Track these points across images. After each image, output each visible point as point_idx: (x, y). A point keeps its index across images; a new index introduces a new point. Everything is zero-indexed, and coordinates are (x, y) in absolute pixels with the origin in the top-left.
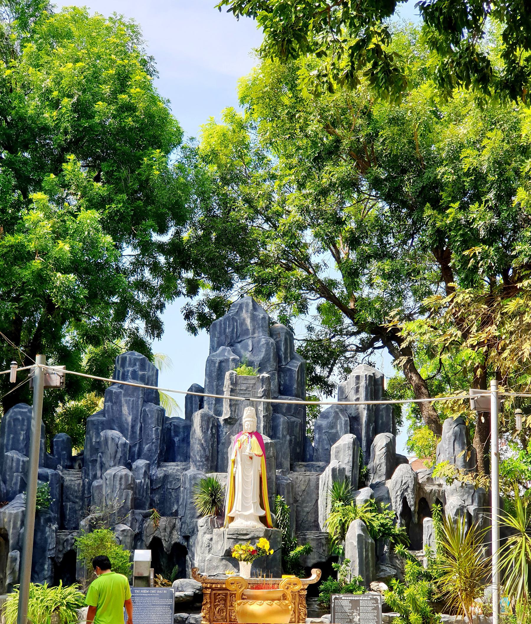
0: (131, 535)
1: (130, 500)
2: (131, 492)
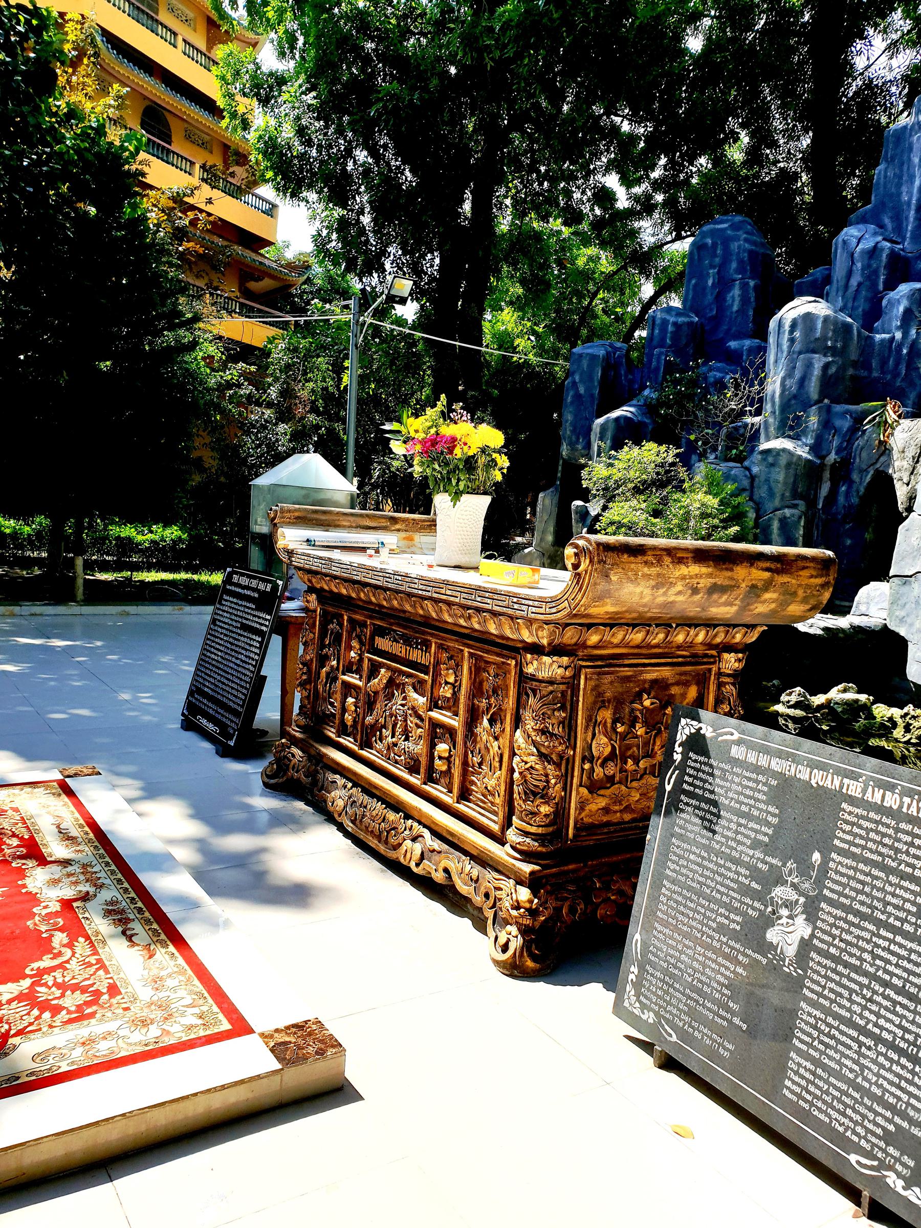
0: (788, 465)
1: (814, 379)
2: (819, 361)
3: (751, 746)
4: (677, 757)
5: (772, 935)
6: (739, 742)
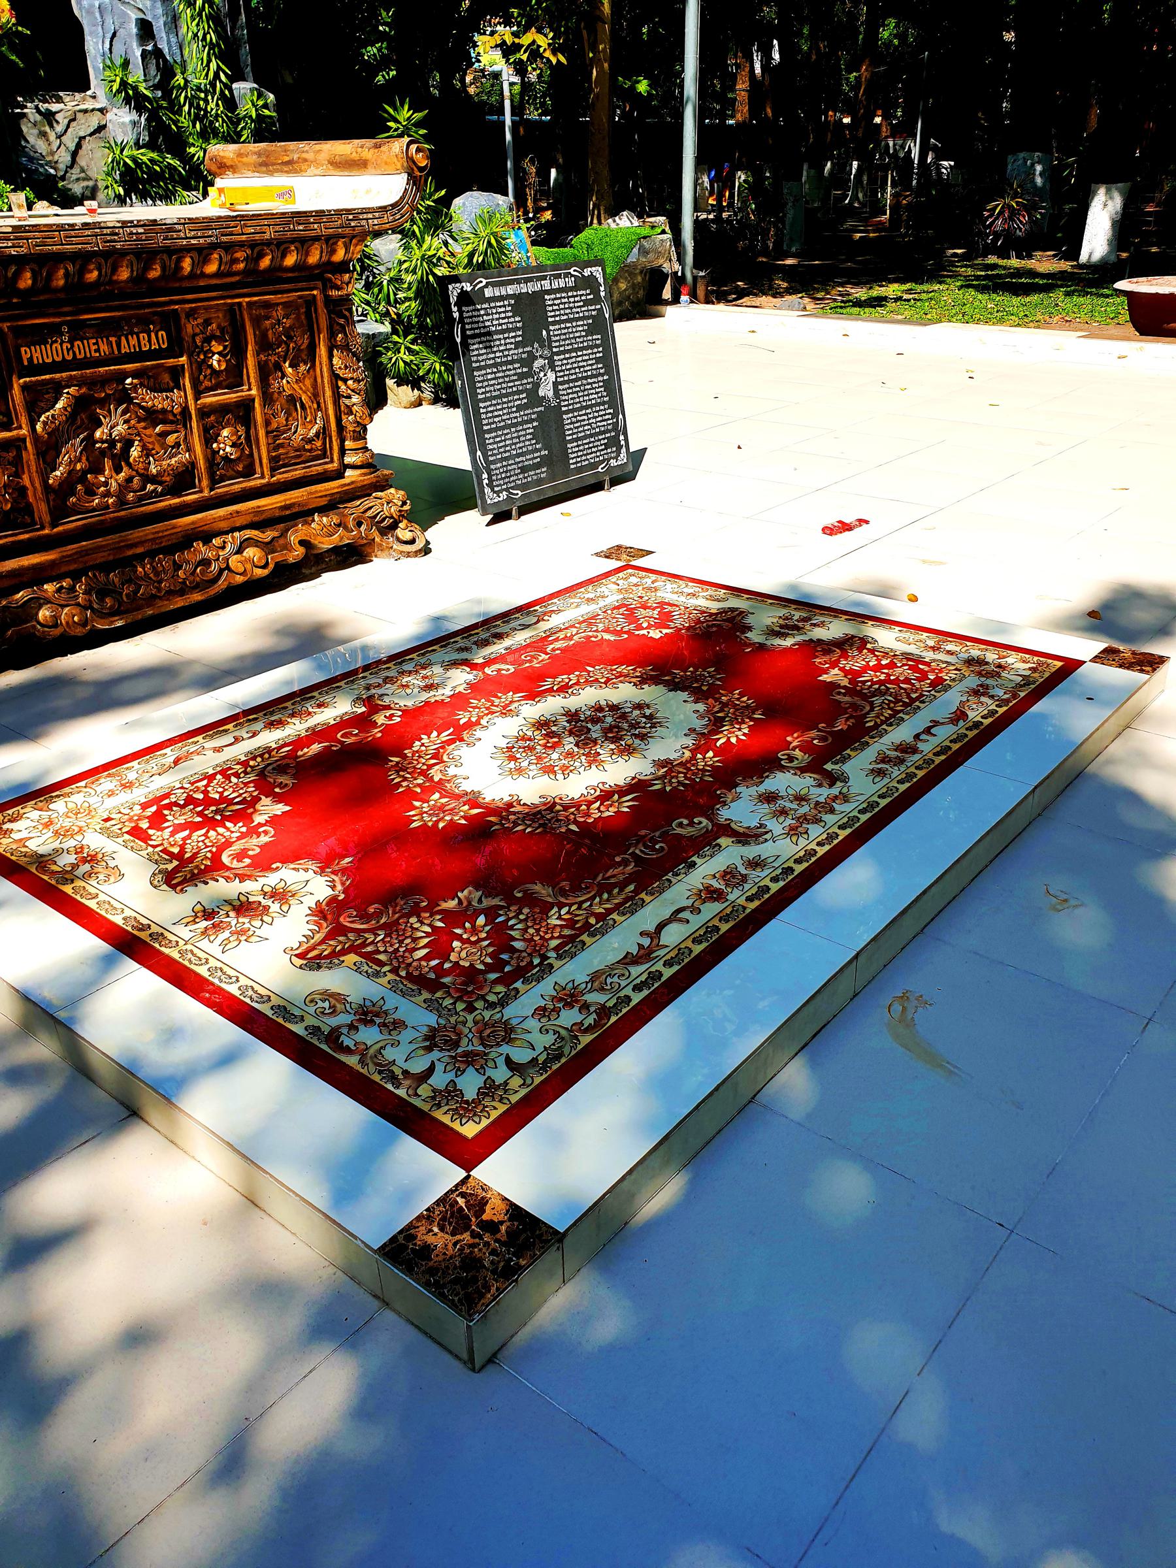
3: (494, 285)
4: (456, 315)
5: (541, 393)
6: (486, 286)
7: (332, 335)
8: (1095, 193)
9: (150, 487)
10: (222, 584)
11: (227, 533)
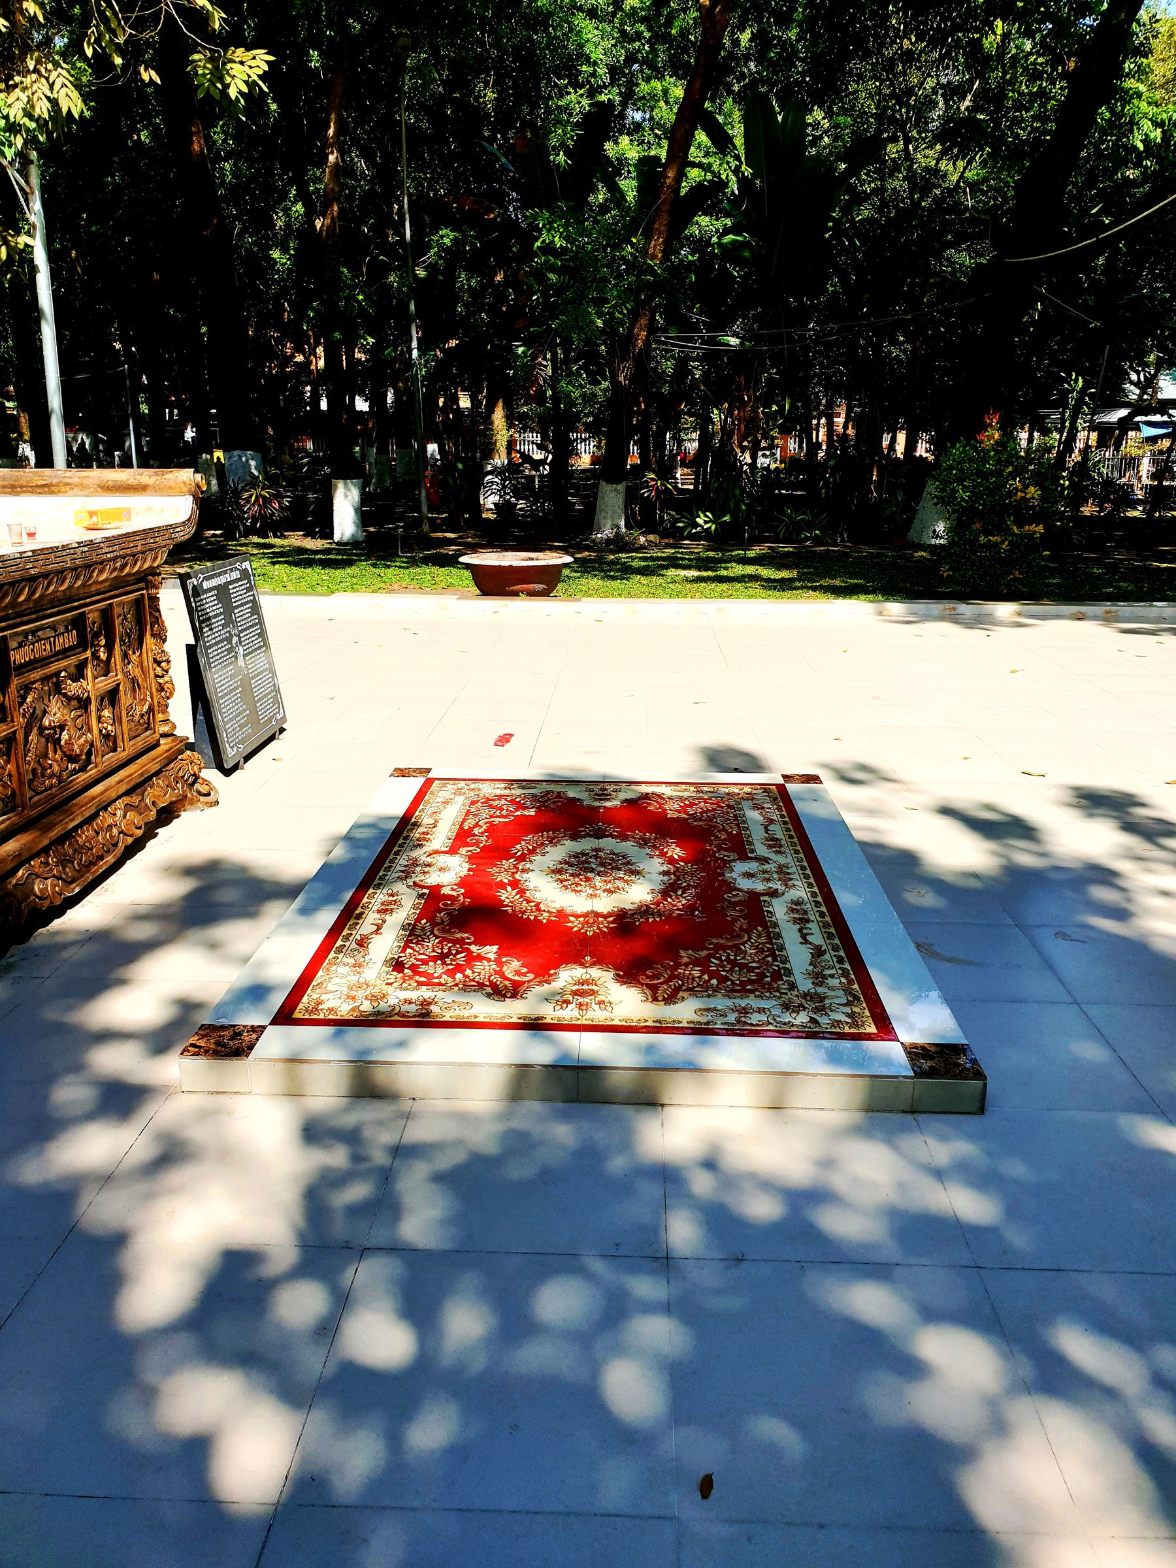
7: (152, 628)
8: (336, 487)
9: (71, 766)
10: (121, 846)
11: (114, 801)
